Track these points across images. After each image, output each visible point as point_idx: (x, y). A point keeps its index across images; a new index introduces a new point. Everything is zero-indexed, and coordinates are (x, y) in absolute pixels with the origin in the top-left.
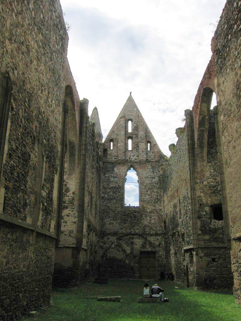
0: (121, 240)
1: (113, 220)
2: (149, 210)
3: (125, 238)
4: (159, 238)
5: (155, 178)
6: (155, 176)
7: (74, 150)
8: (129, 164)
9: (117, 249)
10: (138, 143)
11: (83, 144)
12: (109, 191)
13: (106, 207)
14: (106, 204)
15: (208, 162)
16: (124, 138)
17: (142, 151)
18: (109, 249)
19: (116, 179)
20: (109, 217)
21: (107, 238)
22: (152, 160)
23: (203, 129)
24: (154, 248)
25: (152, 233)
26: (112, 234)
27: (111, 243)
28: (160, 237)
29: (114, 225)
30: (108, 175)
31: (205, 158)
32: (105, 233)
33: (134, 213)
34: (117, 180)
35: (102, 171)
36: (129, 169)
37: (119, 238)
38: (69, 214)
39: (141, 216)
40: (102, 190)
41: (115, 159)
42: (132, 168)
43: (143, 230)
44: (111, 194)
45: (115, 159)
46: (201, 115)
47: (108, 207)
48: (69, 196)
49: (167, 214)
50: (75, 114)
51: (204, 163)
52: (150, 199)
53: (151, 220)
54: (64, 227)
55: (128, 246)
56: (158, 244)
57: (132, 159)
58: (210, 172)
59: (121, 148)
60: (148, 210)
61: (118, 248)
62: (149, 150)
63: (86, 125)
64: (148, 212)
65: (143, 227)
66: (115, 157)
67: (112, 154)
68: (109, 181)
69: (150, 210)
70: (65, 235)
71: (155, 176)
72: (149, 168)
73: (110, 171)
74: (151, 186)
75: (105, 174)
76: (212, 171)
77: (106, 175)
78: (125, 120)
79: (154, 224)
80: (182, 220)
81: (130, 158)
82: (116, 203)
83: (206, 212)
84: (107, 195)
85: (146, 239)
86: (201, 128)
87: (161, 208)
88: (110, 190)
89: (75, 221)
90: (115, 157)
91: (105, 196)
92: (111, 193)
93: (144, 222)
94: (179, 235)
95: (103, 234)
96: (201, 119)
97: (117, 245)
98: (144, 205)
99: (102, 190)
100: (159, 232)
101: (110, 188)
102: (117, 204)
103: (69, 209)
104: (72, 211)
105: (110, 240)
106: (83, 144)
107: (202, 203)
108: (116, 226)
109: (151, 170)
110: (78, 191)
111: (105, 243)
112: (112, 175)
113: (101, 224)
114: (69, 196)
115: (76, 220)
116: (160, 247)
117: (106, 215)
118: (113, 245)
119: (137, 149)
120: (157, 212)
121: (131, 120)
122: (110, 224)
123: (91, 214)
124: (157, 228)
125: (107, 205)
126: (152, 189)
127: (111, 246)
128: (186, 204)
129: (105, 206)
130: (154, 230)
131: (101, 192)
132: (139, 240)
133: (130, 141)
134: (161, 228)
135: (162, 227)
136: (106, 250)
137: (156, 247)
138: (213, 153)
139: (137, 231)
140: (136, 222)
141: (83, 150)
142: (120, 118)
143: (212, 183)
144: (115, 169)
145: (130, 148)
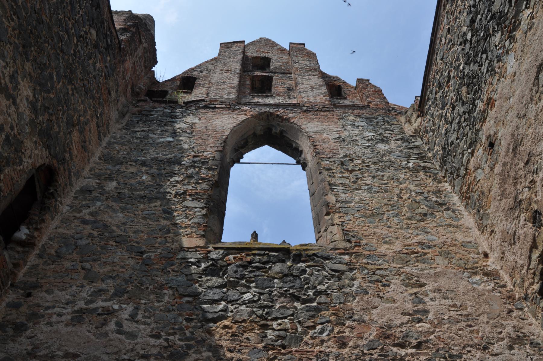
1: (118, 293)
29: (112, 326)
40: (92, 165)
44: (142, 183)
53: (421, 301)
69: (397, 247)
108: (132, 336)
120: (446, 255)
140: (309, 309)
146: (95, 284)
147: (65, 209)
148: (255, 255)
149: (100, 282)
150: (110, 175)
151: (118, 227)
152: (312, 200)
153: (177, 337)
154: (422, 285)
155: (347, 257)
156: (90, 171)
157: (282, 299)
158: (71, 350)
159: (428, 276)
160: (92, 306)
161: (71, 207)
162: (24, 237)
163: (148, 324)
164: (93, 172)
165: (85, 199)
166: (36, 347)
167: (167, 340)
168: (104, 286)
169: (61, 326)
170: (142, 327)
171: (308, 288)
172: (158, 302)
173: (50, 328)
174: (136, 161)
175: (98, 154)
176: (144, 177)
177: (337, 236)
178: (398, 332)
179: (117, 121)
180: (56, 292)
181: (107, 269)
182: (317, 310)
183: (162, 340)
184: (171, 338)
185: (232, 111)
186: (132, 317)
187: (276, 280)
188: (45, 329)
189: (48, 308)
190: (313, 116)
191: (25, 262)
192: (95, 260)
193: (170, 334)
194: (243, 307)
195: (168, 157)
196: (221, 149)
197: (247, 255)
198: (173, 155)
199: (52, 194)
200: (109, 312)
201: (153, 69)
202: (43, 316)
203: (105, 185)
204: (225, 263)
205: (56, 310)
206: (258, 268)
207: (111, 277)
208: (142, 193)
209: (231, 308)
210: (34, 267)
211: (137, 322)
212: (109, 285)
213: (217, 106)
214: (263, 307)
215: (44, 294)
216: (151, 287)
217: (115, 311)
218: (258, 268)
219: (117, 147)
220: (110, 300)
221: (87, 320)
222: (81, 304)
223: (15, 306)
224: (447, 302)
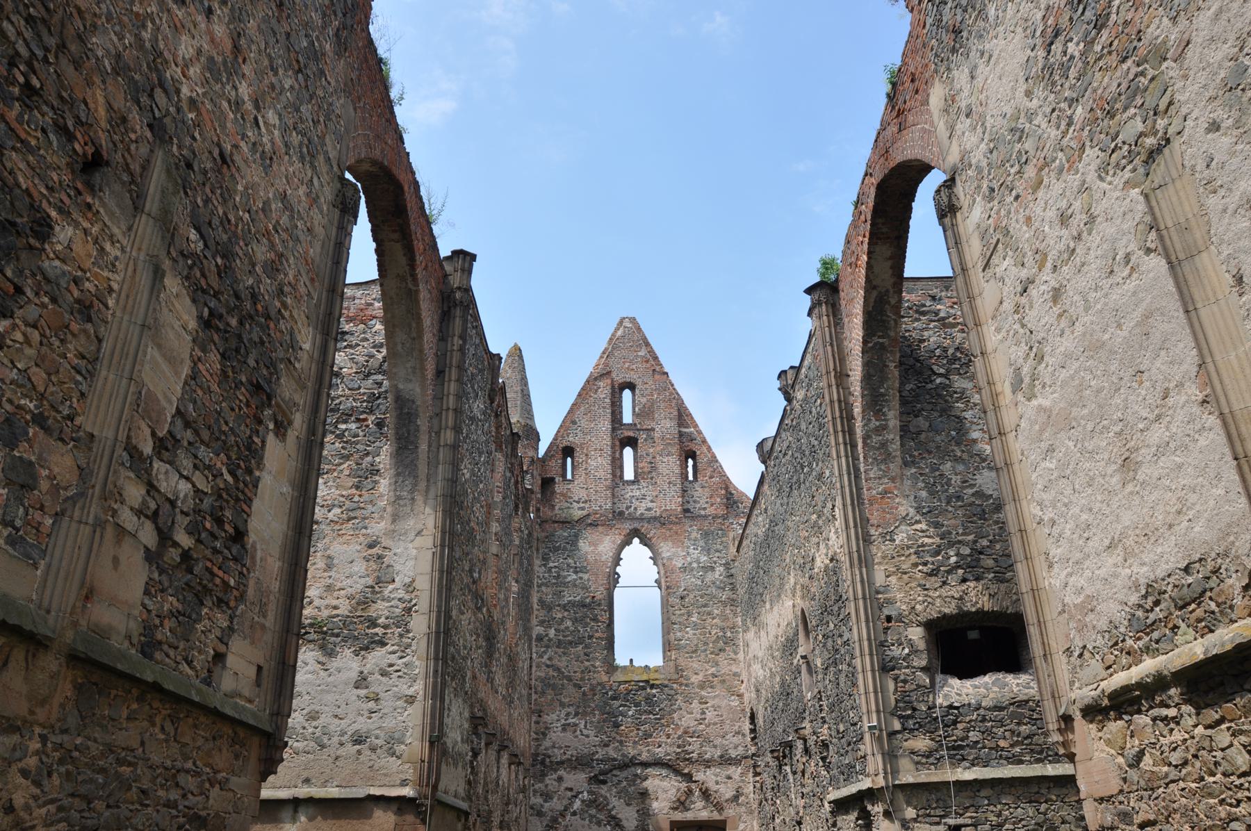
0: (604, 782)
1: (576, 714)
2: (695, 676)
3: (616, 776)
4: (735, 772)
5: (713, 569)
7: (412, 428)
8: (628, 526)
9: (591, 816)
10: (654, 458)
11: (448, 409)
12: (559, 616)
13: (551, 670)
14: (550, 659)
15: (906, 464)
16: (606, 440)
17: (670, 483)
18: (563, 816)
19: (586, 576)
20: (562, 705)
21: (555, 776)
22: (703, 512)
23: (881, 340)
24: (719, 807)
25: (707, 756)
26: (575, 764)
27: (569, 794)
28: (739, 770)
29: (578, 732)
31: (895, 447)
32: (548, 760)
33: (648, 690)
34: (589, 580)
35: (538, 550)
36: (628, 542)
37: (596, 776)
38: (391, 665)
39: (671, 698)
40: (536, 612)
41: (579, 508)
42: (636, 540)
43: (679, 747)
44: (567, 628)
45: (579, 508)
46: (875, 288)
47: (558, 670)
48: (389, 600)
49: (761, 684)
50: (417, 292)
51: (891, 465)
52: (698, 639)
53: (703, 713)
54: (370, 718)
55: (628, 805)
56: (729, 794)
57: (635, 509)
58: (915, 497)
59: (601, 474)
61: (593, 812)
62: (691, 478)
63: (461, 342)
65: (679, 738)
66: (582, 505)
67: (569, 494)
68: (560, 582)
69: (700, 677)
70: (373, 749)
71: (715, 563)
72: (694, 535)
73: (565, 549)
75: (545, 559)
76: (924, 494)
77: (551, 565)
78: (613, 387)
79: (715, 724)
80: (819, 692)
81: (628, 508)
82: (586, 654)
83: (911, 643)
85: (688, 777)
86: (876, 339)
87: (738, 670)
88: (566, 614)
89: (411, 692)
90: (578, 502)
91: (547, 635)
92: (569, 623)
93: (680, 719)
94: (807, 751)
95: (543, 762)
96: (872, 304)
97: (590, 801)
99: (537, 613)
100: (733, 754)
101: (564, 607)
102: (588, 660)
103: (389, 648)
104: (401, 658)
105: (564, 785)
106: (448, 409)
107: (894, 614)
108: (587, 736)
109: (702, 543)
110: (428, 577)
111: (547, 796)
112: (570, 561)
113: (533, 729)
114: (389, 600)
115: (418, 687)
116: (738, 805)
117: (549, 697)
118: (577, 804)
119: (652, 478)
121: (632, 387)
122: (565, 728)
123: (490, 680)
124: (727, 737)
125: (555, 662)
126: (705, 606)
127: (571, 804)
128: (832, 626)
129: (548, 666)
130: (715, 747)
131: (534, 621)
132: (665, 784)
133: (628, 452)
134: (736, 740)
135: (744, 735)
136: (555, 820)
137: (725, 804)
138: (919, 433)
139: (660, 752)
140: (656, 719)
141: (447, 427)
142: (596, 379)
143: (927, 540)
144: (581, 544)
145: (629, 474)
154: (707, 703)
155: (675, 686)
159: (710, 697)
174: (559, 605)
178: (691, 730)
182: (659, 719)
186: (585, 726)
190: (668, 533)
195: (577, 599)
200: (576, 725)
210: (536, 700)
212: (571, 710)
219: (543, 588)
222: (563, 721)
223: (537, 723)
224: (716, 713)
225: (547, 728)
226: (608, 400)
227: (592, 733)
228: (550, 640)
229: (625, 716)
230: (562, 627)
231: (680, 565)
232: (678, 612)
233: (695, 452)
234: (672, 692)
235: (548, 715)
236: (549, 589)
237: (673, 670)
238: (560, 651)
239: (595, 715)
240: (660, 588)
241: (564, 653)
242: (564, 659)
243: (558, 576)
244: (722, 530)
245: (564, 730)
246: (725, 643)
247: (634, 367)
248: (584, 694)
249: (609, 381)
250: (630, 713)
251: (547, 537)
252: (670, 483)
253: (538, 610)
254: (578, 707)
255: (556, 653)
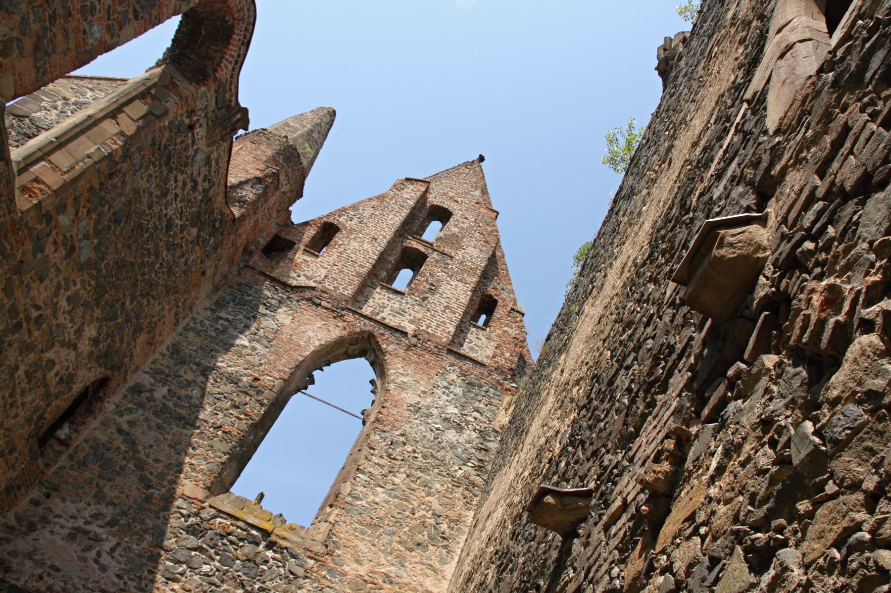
1: (112, 523)
2: (355, 565)
6: (467, 423)
12: (190, 376)
13: (121, 438)
14: (131, 423)
20: (100, 497)
29: (93, 554)
30: (230, 317)
35: (216, 289)
40: (157, 356)
60: (351, 568)
64: (344, 574)
69: (363, 570)
74: (425, 457)
75: (220, 304)
77: (223, 315)
84: (169, 390)
91: (151, 391)
98: (342, 528)
108: (104, 569)
109: (459, 391)
117: (87, 475)
125: (137, 432)
129: (120, 431)
146: (99, 506)
147: (110, 407)
148: (238, 527)
149: (104, 505)
150: (167, 376)
151: (145, 448)
152: (339, 474)
153: (134, 584)
156: (152, 363)
157: (231, 582)
158: (57, 564)
160: (88, 528)
161: (117, 406)
162: (63, 437)
163: (120, 563)
164: (153, 366)
165: (131, 402)
166: (36, 550)
167: (125, 583)
168: (105, 511)
169: (57, 538)
170: (113, 563)
171: (259, 580)
172: (138, 545)
173: (51, 537)
174: (198, 365)
175: (169, 340)
176: (194, 392)
177: (320, 536)
179: (208, 296)
180: (68, 502)
181: (115, 493)
183: (122, 582)
184: (130, 583)
185: (335, 318)
186: (113, 550)
187: (238, 562)
188: (48, 536)
189: (57, 516)
190: (414, 358)
191: (56, 461)
192: (109, 480)
193: (130, 579)
194: (196, 577)
195: (230, 369)
196: (286, 377)
197: (232, 524)
198: (237, 368)
199: (100, 398)
200: (97, 539)
201: (290, 208)
202: (50, 523)
203: (157, 389)
204: (207, 526)
205: (62, 521)
206: (232, 543)
207: (114, 503)
208: (183, 412)
209: (188, 573)
210: (62, 468)
211: (113, 557)
212: (109, 512)
213: (323, 303)
214: (212, 584)
215: (58, 500)
216: (139, 527)
217: (102, 540)
218: (232, 543)
219: (191, 335)
220: (102, 527)
221: (78, 540)
222: (80, 523)
223: (35, 503)
225: (44, 520)
226: (412, 203)
227: (114, 567)
228: (151, 399)
229: (192, 569)
230: (183, 393)
231: (413, 403)
232: (375, 459)
233: (495, 302)
234: (300, 571)
235: (63, 500)
236: (198, 339)
237: (320, 537)
238: (155, 421)
239: (142, 539)
240: (364, 423)
241: (159, 427)
242: (153, 433)
243: (224, 331)
244: (496, 389)
245: (71, 537)
246: (430, 537)
247: (459, 200)
248: (148, 499)
249: (423, 189)
250: (206, 568)
251: (240, 285)
252: (447, 307)
253: (164, 355)
254: (124, 513)
255: (147, 420)
